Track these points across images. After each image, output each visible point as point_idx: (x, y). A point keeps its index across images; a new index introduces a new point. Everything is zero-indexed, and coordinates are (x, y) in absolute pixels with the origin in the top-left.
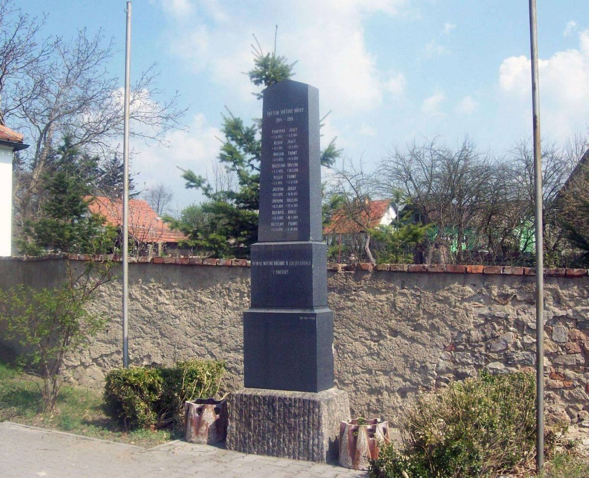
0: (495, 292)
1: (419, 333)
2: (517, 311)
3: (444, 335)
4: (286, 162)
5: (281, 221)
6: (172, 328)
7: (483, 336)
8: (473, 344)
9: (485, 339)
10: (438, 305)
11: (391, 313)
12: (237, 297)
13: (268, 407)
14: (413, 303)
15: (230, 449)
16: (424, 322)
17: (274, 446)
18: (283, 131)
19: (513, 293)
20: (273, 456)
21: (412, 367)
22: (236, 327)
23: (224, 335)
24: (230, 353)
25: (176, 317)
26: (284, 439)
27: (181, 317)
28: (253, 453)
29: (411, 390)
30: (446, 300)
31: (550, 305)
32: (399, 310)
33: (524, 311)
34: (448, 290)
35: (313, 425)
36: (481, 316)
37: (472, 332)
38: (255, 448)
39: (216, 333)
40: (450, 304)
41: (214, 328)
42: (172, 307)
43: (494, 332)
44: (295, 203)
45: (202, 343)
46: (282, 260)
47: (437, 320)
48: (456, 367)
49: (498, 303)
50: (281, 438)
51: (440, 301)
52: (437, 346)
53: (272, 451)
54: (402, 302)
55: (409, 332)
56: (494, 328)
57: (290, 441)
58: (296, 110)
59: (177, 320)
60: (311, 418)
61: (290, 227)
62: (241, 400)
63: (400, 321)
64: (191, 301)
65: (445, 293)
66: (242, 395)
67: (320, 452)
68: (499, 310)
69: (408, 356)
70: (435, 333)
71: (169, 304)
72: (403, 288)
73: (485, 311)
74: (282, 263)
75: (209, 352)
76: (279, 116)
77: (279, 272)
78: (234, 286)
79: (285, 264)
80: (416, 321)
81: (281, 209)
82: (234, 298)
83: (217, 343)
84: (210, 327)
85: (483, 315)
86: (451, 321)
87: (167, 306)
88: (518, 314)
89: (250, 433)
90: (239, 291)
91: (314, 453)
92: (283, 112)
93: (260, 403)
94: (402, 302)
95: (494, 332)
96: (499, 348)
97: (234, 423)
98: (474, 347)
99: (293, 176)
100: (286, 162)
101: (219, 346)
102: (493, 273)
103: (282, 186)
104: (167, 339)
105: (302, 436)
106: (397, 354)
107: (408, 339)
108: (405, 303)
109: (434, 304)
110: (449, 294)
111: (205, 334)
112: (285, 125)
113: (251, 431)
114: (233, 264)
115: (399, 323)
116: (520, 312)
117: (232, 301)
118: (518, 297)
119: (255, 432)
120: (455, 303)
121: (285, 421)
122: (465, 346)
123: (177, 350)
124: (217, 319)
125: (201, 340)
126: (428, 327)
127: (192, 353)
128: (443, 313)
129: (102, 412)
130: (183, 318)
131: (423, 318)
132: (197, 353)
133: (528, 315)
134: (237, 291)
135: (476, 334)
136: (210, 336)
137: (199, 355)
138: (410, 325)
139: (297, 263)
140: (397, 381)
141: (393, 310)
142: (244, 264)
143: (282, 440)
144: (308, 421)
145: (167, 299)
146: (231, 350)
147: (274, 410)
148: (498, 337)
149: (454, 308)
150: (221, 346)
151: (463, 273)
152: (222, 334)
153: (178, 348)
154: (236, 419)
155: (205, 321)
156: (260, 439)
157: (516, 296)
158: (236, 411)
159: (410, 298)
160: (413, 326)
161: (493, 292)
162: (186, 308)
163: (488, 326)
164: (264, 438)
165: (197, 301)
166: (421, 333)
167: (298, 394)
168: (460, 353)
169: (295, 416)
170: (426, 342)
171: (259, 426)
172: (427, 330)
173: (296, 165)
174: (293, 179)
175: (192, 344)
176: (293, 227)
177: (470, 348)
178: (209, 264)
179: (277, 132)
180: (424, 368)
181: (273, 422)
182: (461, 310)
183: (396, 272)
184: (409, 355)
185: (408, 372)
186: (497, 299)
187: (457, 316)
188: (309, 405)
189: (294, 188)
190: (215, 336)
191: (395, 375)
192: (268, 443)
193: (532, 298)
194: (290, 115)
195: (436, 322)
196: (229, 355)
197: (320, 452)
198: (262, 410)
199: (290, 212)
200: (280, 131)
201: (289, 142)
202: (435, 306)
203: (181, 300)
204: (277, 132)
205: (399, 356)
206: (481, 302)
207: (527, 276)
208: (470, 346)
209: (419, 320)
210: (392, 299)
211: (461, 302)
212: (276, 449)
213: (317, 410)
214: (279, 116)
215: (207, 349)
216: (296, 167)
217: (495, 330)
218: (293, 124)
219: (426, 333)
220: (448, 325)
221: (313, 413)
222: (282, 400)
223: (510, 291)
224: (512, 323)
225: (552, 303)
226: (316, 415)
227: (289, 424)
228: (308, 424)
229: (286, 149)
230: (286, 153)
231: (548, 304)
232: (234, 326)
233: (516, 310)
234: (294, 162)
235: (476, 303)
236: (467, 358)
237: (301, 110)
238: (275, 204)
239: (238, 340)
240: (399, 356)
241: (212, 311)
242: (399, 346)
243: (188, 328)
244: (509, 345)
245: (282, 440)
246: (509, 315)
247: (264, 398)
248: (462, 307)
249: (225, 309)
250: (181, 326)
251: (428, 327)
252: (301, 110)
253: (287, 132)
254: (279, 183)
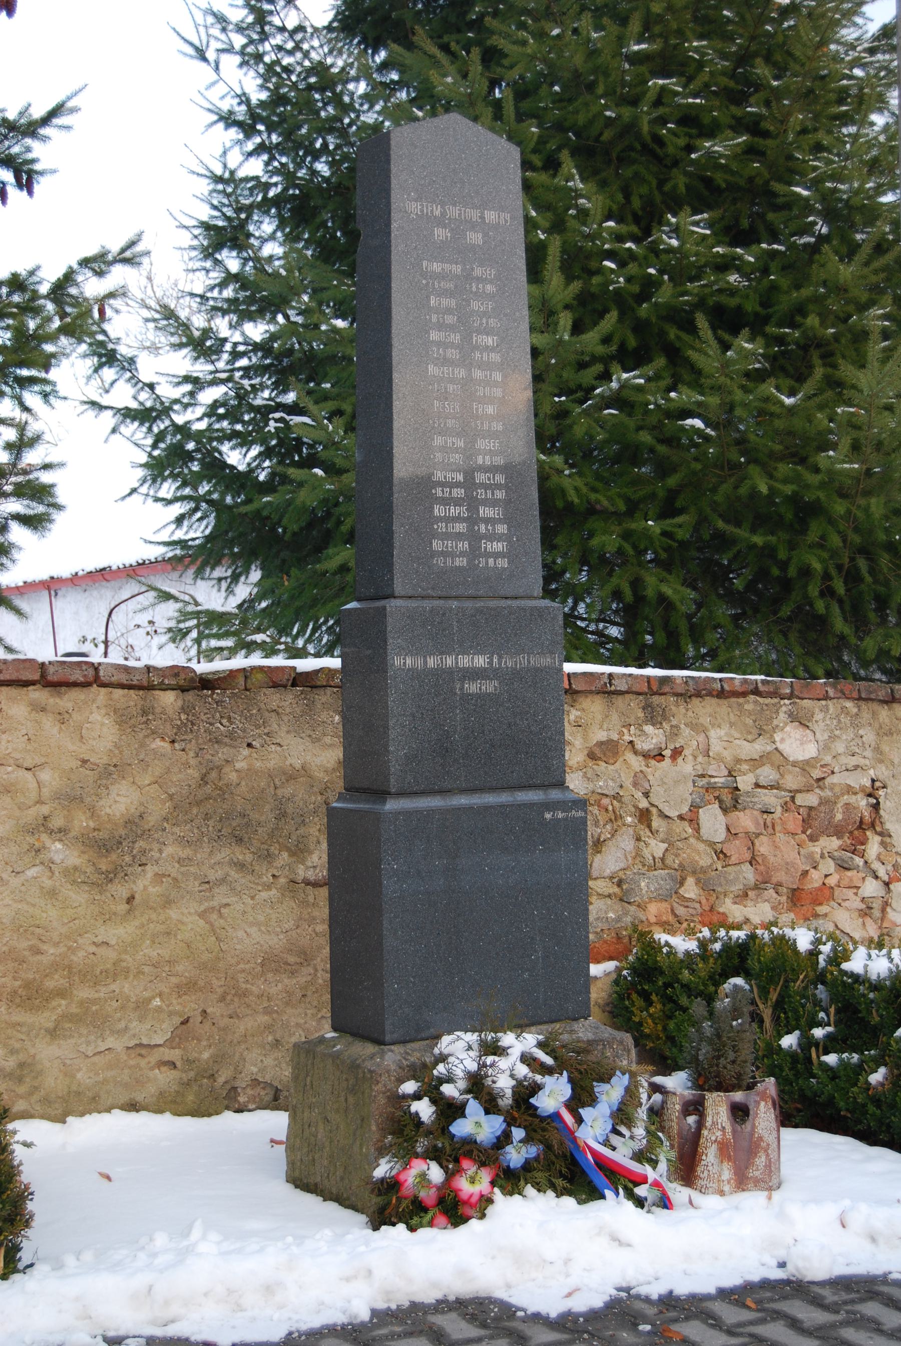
5: (459, 536)
18: (457, 269)
44: (498, 486)
61: (488, 555)
74: (480, 661)
77: (472, 688)
79: (490, 663)
81: (457, 502)
92: (453, 212)
176: (496, 555)
179: (436, 267)
193: (663, 746)
199: (485, 512)
204: (436, 267)
214: (441, 222)
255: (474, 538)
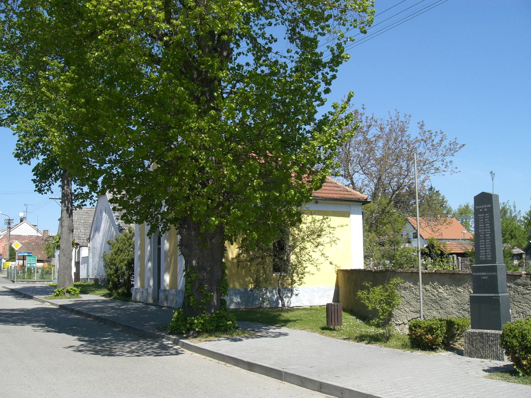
18: (483, 215)
25: (448, 299)
42: (445, 294)
58: (488, 206)
64: (454, 291)
74: (485, 274)
76: (481, 209)
77: (484, 278)
92: (482, 207)
130: (451, 300)
167: (493, 331)
169: (492, 341)
179: (480, 215)
194: (485, 208)
199: (488, 251)
204: (480, 215)
218: (487, 212)
222: (486, 334)
229: (484, 224)
255: (486, 255)
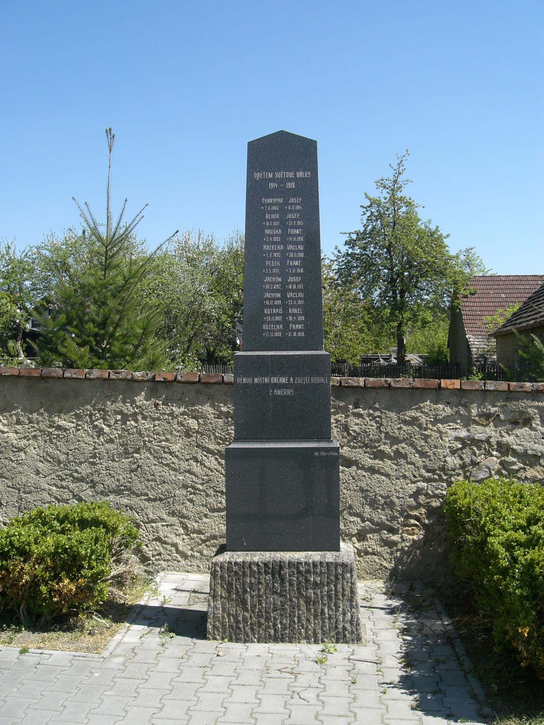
0: (474, 412)
1: (381, 462)
2: (500, 432)
3: (413, 464)
4: (284, 242)
5: (278, 323)
6: (13, 465)
7: (461, 462)
8: (450, 472)
9: (463, 467)
10: (405, 428)
11: (343, 438)
12: (116, 422)
13: (273, 577)
14: (372, 426)
15: (215, 639)
16: (386, 448)
17: (284, 628)
18: (280, 200)
19: (496, 412)
20: (282, 641)
21: (373, 504)
22: (117, 462)
23: (98, 472)
24: (109, 496)
25: (20, 450)
26: (299, 618)
27: (27, 450)
28: (252, 642)
29: (372, 531)
30: (414, 421)
31: (538, 425)
32: (353, 434)
33: (507, 433)
34: (416, 409)
35: (343, 595)
36: (457, 439)
37: (448, 459)
38: (254, 634)
39: (85, 470)
40: (420, 426)
41: (81, 463)
42: (12, 435)
43: (474, 458)
44: (300, 299)
45: (64, 483)
46: (284, 376)
47: (403, 445)
48: (428, 500)
49: (478, 424)
50: (294, 616)
51: (405, 422)
52: (405, 477)
53: (282, 635)
54: (357, 424)
55: (369, 461)
56: (474, 454)
57: (308, 620)
58: (300, 174)
59: (22, 454)
60: (339, 586)
61: (293, 331)
62: (230, 570)
63: (354, 447)
64: (42, 426)
65: (413, 413)
66: (230, 563)
67: (354, 630)
68: (480, 432)
69: (367, 490)
70: (402, 461)
71: (8, 432)
72: (356, 407)
73: (463, 433)
74: (283, 380)
75: (74, 496)
76: (273, 180)
77: (279, 392)
78: (110, 406)
79: (289, 381)
80: (376, 447)
81: (277, 307)
82: (112, 422)
83: (87, 483)
84: (75, 462)
85: (460, 438)
86: (422, 446)
87: (6, 435)
88: (502, 436)
89: (246, 614)
90: (121, 413)
91: (347, 632)
92: (278, 175)
93: (259, 573)
94: (357, 424)
95: (474, 458)
96: (481, 476)
97: (219, 602)
98: (451, 476)
99: (296, 263)
100: (284, 242)
101: (91, 487)
102: (474, 388)
103: (278, 276)
104: (6, 481)
105: (326, 610)
106: (352, 488)
107: (366, 470)
108: (361, 425)
109: (399, 426)
110: (419, 414)
111: (68, 472)
112: (285, 193)
113: (248, 611)
114: (112, 376)
115: (354, 450)
116: (504, 434)
117: (109, 426)
118: (502, 417)
119: (253, 612)
120: (427, 424)
121: (300, 593)
122: (440, 476)
123: (24, 496)
124: (86, 451)
125: (62, 480)
126: (392, 454)
127: (48, 498)
128: (412, 437)
129: (128, 625)
130: (32, 451)
131: (385, 444)
132: (56, 498)
133: (512, 437)
134: (117, 413)
135: (452, 461)
136: (75, 474)
137: (59, 500)
138: (368, 452)
139: (306, 380)
140: (353, 522)
141: (345, 434)
142: (129, 377)
143: (296, 619)
144: (336, 590)
145: (4, 425)
146: (110, 491)
147: (283, 580)
148: (478, 463)
149: (424, 431)
150: (94, 488)
151: (435, 389)
152: (96, 471)
153: (25, 492)
154: (222, 597)
155: (67, 454)
156: (262, 621)
157: (499, 415)
158: (222, 587)
159: (367, 419)
160: (373, 453)
161: (473, 411)
162: (35, 437)
163: (467, 450)
164: (268, 619)
165: (54, 427)
166: (383, 461)
167: (315, 556)
168: (434, 484)
169: (316, 585)
170: (390, 472)
171: (260, 603)
172: (390, 458)
173: (301, 248)
174: (296, 267)
175: (47, 486)
176: (298, 331)
177: (445, 478)
178: (74, 376)
179: (270, 201)
180: (391, 505)
181: (282, 596)
182: (434, 434)
183: (348, 387)
184: (369, 489)
185: (367, 509)
186: (477, 418)
187: (429, 440)
188: (336, 570)
189: (298, 279)
190: (84, 473)
191: (351, 514)
192: (275, 625)
193: (518, 417)
194: (290, 180)
195: (403, 448)
196: (107, 498)
197: (354, 630)
198: (263, 581)
200: (275, 200)
201: (290, 216)
202: (400, 429)
203: (27, 426)
204: (270, 201)
205: (355, 490)
206: (457, 423)
207: (512, 392)
208: (445, 474)
209: (379, 446)
210: (343, 421)
211: (434, 424)
212: (287, 632)
213: (348, 575)
214: (273, 180)
215: (71, 492)
216: (301, 251)
217: (475, 455)
218: (293, 193)
219: (389, 462)
220: (418, 452)
221: (343, 578)
222: (295, 565)
223: (493, 410)
224: (495, 447)
225: (539, 422)
226: (347, 582)
227: (307, 597)
228: (336, 595)
229: (284, 225)
230: (285, 231)
231: (535, 423)
232: (113, 460)
233: (498, 431)
234: (297, 243)
235: (451, 424)
236: (442, 490)
237: (307, 174)
238: (267, 299)
239: (121, 478)
240: (355, 490)
241: (79, 441)
242: (354, 479)
243: (40, 465)
244: (493, 472)
245: (296, 619)
246: (491, 437)
247: (266, 565)
248: (435, 429)
249: (99, 437)
250: (30, 462)
251: (392, 454)
252: (307, 174)
253: (286, 203)
254: (275, 271)
255: (286, 324)
